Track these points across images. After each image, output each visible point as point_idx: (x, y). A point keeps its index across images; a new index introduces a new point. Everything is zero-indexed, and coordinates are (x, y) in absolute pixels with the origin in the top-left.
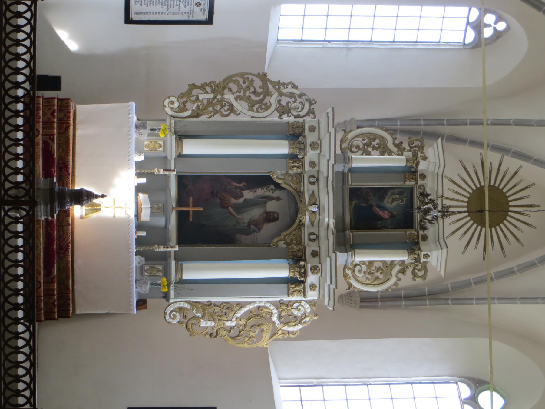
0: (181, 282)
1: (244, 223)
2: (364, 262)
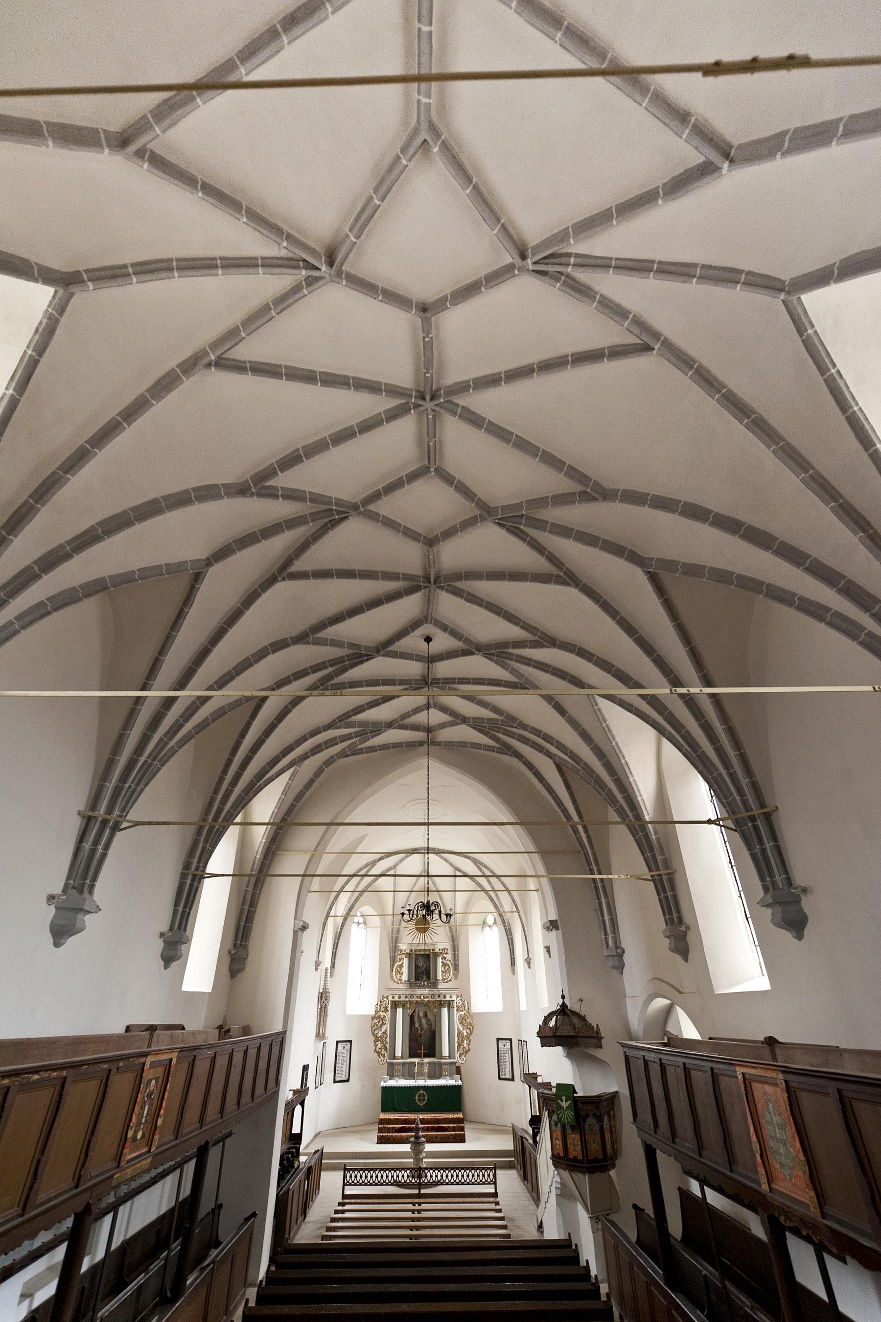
0: (450, 1057)
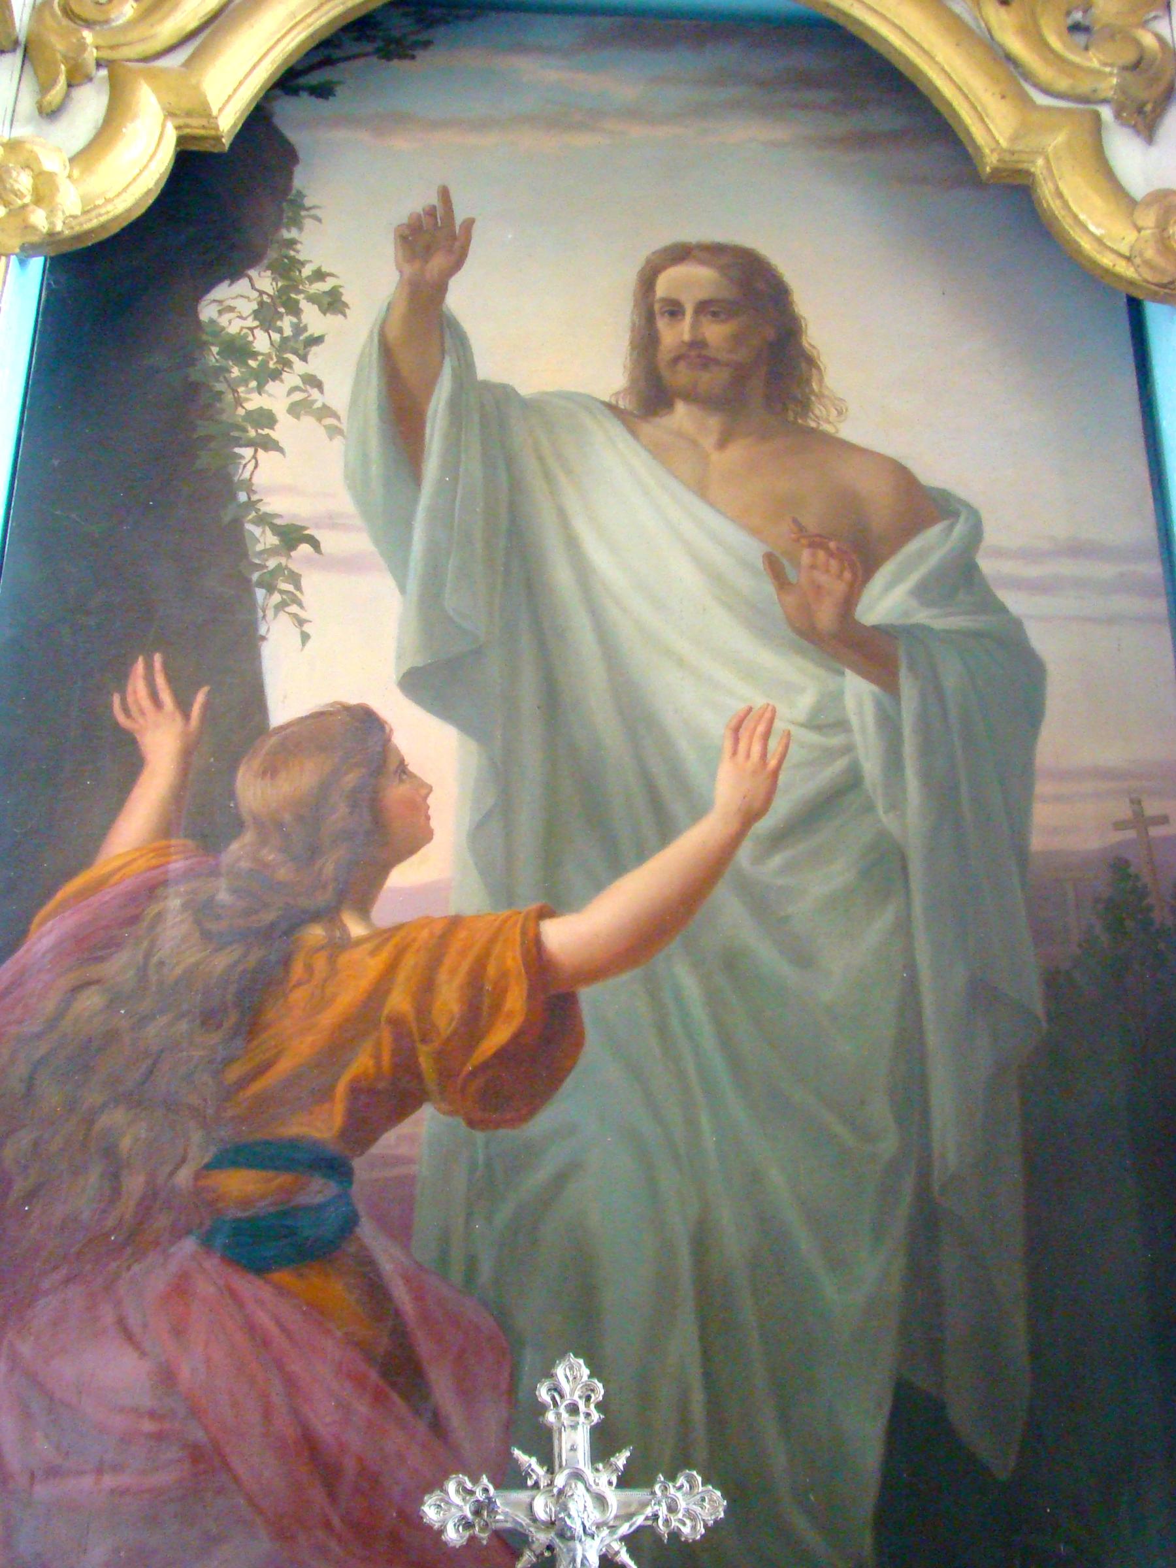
1: (827, 719)
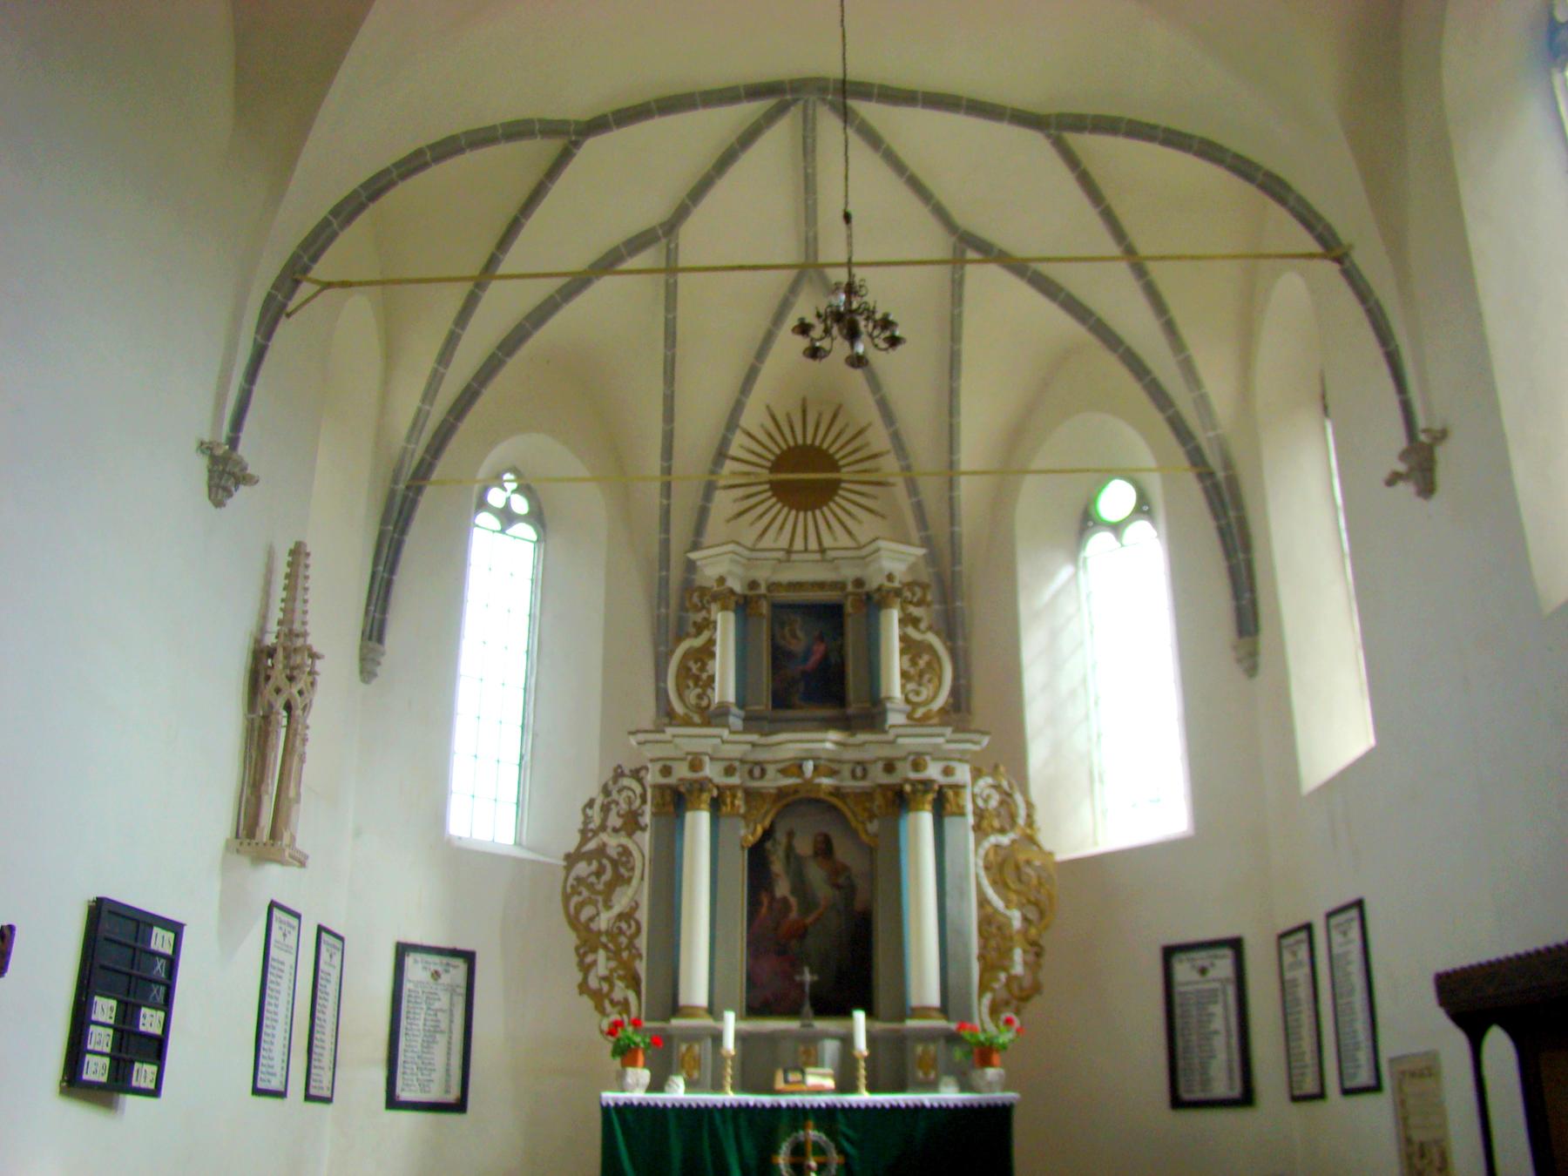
0: (944, 1010)
2: (903, 686)
